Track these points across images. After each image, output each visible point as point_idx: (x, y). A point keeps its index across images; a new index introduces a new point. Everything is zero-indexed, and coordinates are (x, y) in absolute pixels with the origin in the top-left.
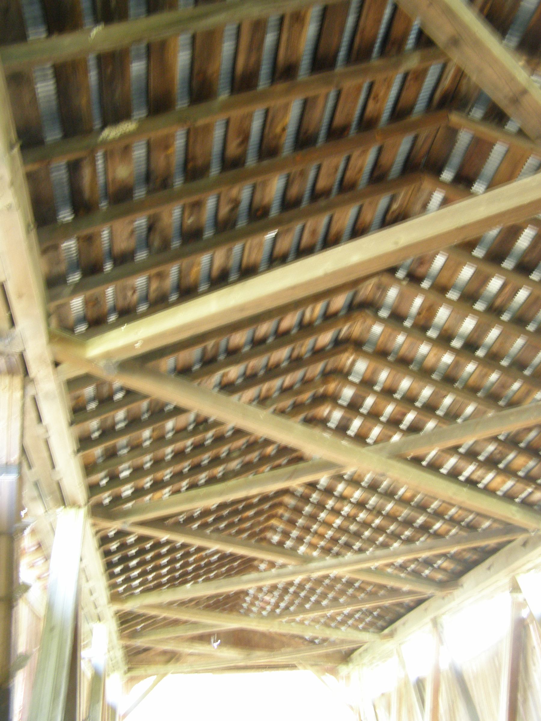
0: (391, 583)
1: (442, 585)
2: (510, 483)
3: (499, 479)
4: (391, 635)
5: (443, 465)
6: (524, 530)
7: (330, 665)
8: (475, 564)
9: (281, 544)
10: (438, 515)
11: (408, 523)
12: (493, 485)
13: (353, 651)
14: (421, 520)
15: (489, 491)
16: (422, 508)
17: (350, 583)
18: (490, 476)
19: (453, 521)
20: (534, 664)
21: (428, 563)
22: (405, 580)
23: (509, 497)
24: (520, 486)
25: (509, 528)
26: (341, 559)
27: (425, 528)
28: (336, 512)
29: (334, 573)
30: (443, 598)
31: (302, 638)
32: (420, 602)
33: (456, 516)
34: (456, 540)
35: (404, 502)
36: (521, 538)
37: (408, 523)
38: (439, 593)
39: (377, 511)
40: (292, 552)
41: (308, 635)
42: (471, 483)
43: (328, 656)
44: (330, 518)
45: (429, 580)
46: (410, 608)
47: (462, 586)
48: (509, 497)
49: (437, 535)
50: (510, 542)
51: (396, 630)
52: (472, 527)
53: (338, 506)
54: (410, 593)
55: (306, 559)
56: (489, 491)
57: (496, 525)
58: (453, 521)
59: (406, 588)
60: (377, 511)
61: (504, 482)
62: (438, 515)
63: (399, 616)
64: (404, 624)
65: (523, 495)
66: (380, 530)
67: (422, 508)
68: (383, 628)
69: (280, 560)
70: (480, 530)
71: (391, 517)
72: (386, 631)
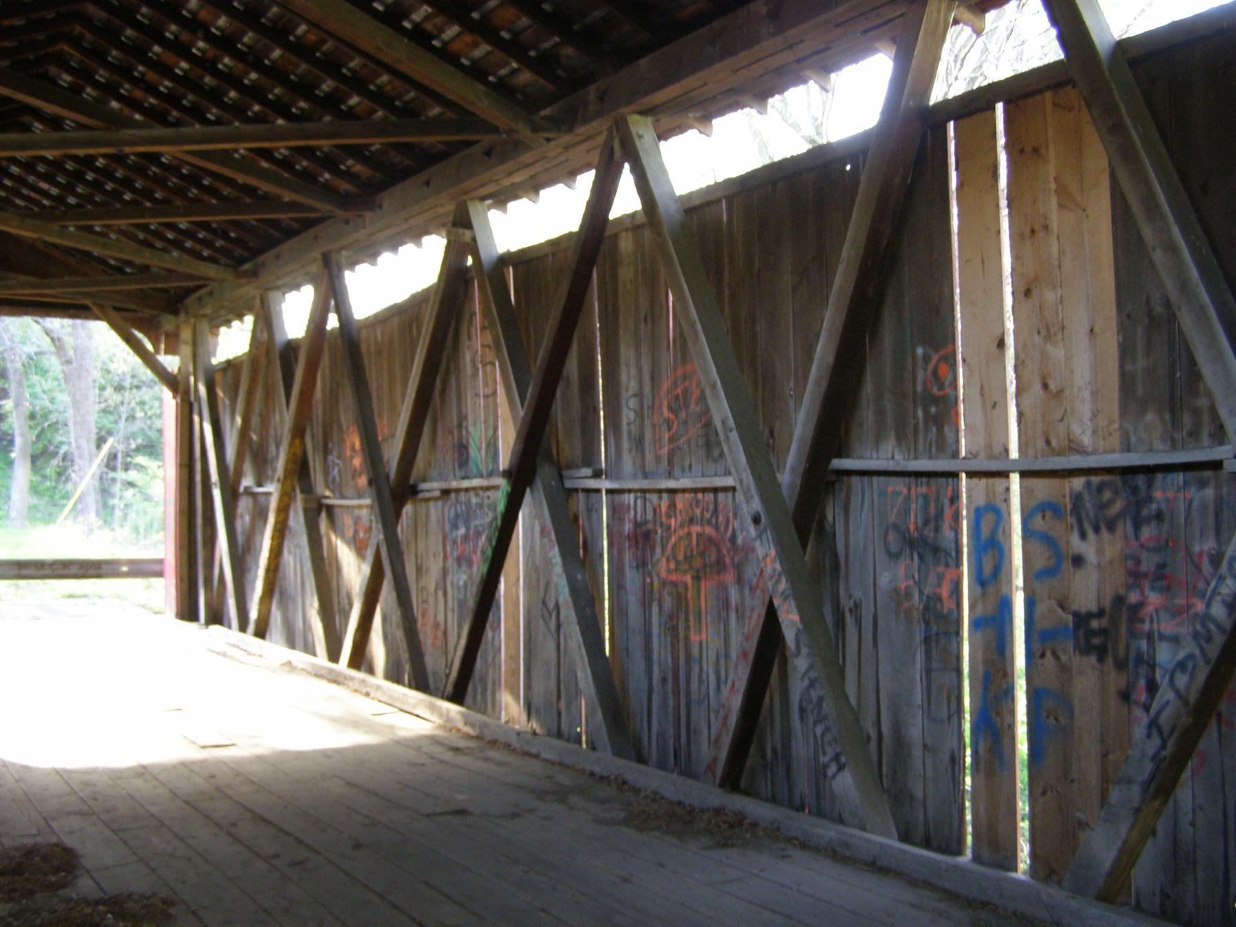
0: (264, 187)
1: (345, 201)
2: (482, 50)
3: (468, 38)
4: (254, 274)
5: (411, 13)
6: (495, 130)
7: (147, 312)
8: (405, 174)
9: (76, 90)
10: (358, 83)
11: (305, 89)
12: (456, 47)
13: (189, 291)
14: (327, 86)
15: (447, 56)
16: (332, 66)
17: (194, 179)
18: (452, 31)
19: (380, 98)
20: (470, 338)
21: (330, 163)
22: (287, 185)
23: (478, 72)
24: (500, 55)
25: (466, 120)
26: (184, 131)
27: (332, 103)
28: (181, 49)
29: (168, 152)
30: (347, 222)
31: (101, 261)
32: (307, 224)
33: (389, 88)
34: (381, 129)
35: (302, 50)
36: (487, 139)
37: (305, 89)
38: (339, 213)
39: (253, 60)
40: (95, 110)
41: (112, 255)
42: (420, 36)
43: (142, 297)
44: (168, 57)
45: (329, 192)
46: (290, 234)
47: (380, 207)
48: (478, 72)
49: (351, 115)
50: (468, 144)
51: (263, 264)
52: (409, 112)
53: (185, 36)
54: (294, 206)
55: (117, 122)
56: (447, 56)
57: (449, 115)
58: (380, 98)
59: (288, 197)
60: (253, 60)
61: (475, 45)
62: (358, 83)
63: (272, 244)
64: (277, 257)
65: (503, 72)
66: (255, 92)
67: (332, 66)
68: (242, 261)
69: (71, 117)
70: (423, 118)
71: (276, 74)
72: (247, 266)
